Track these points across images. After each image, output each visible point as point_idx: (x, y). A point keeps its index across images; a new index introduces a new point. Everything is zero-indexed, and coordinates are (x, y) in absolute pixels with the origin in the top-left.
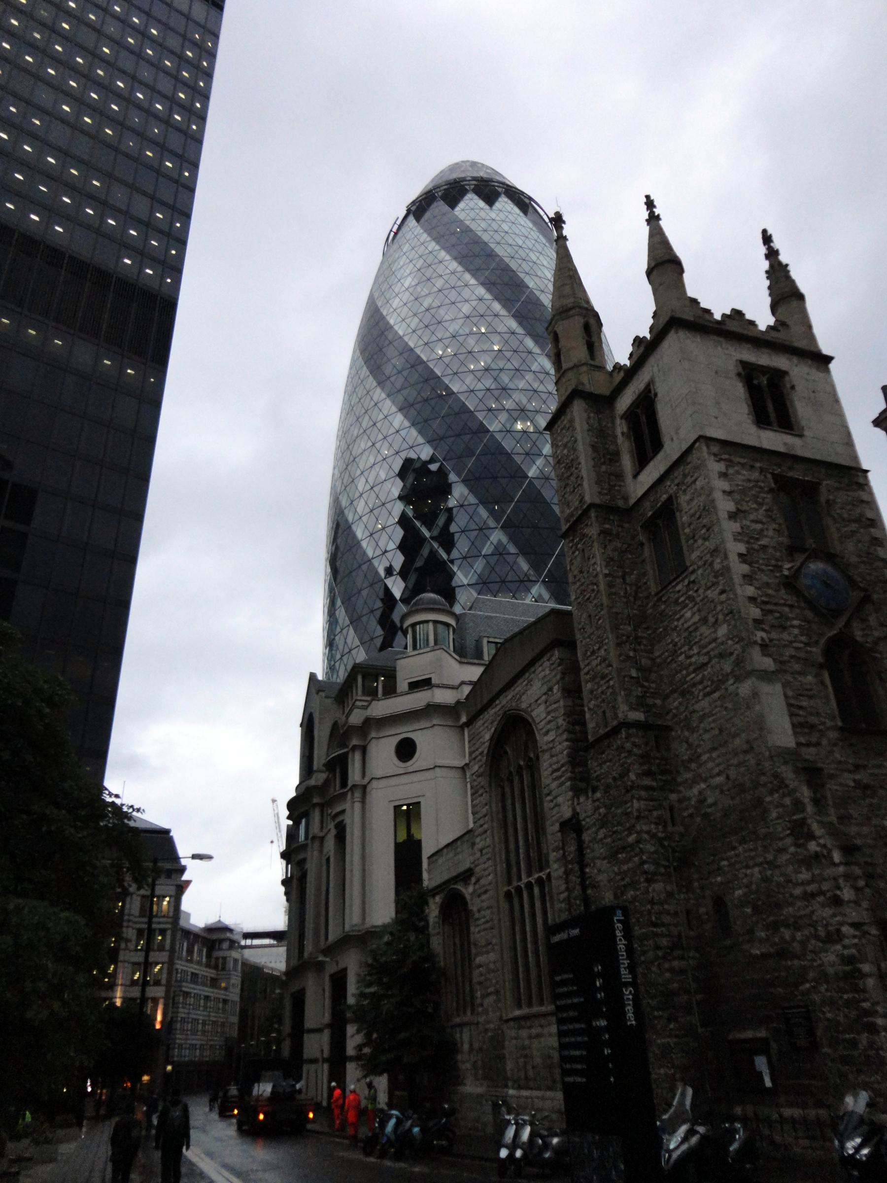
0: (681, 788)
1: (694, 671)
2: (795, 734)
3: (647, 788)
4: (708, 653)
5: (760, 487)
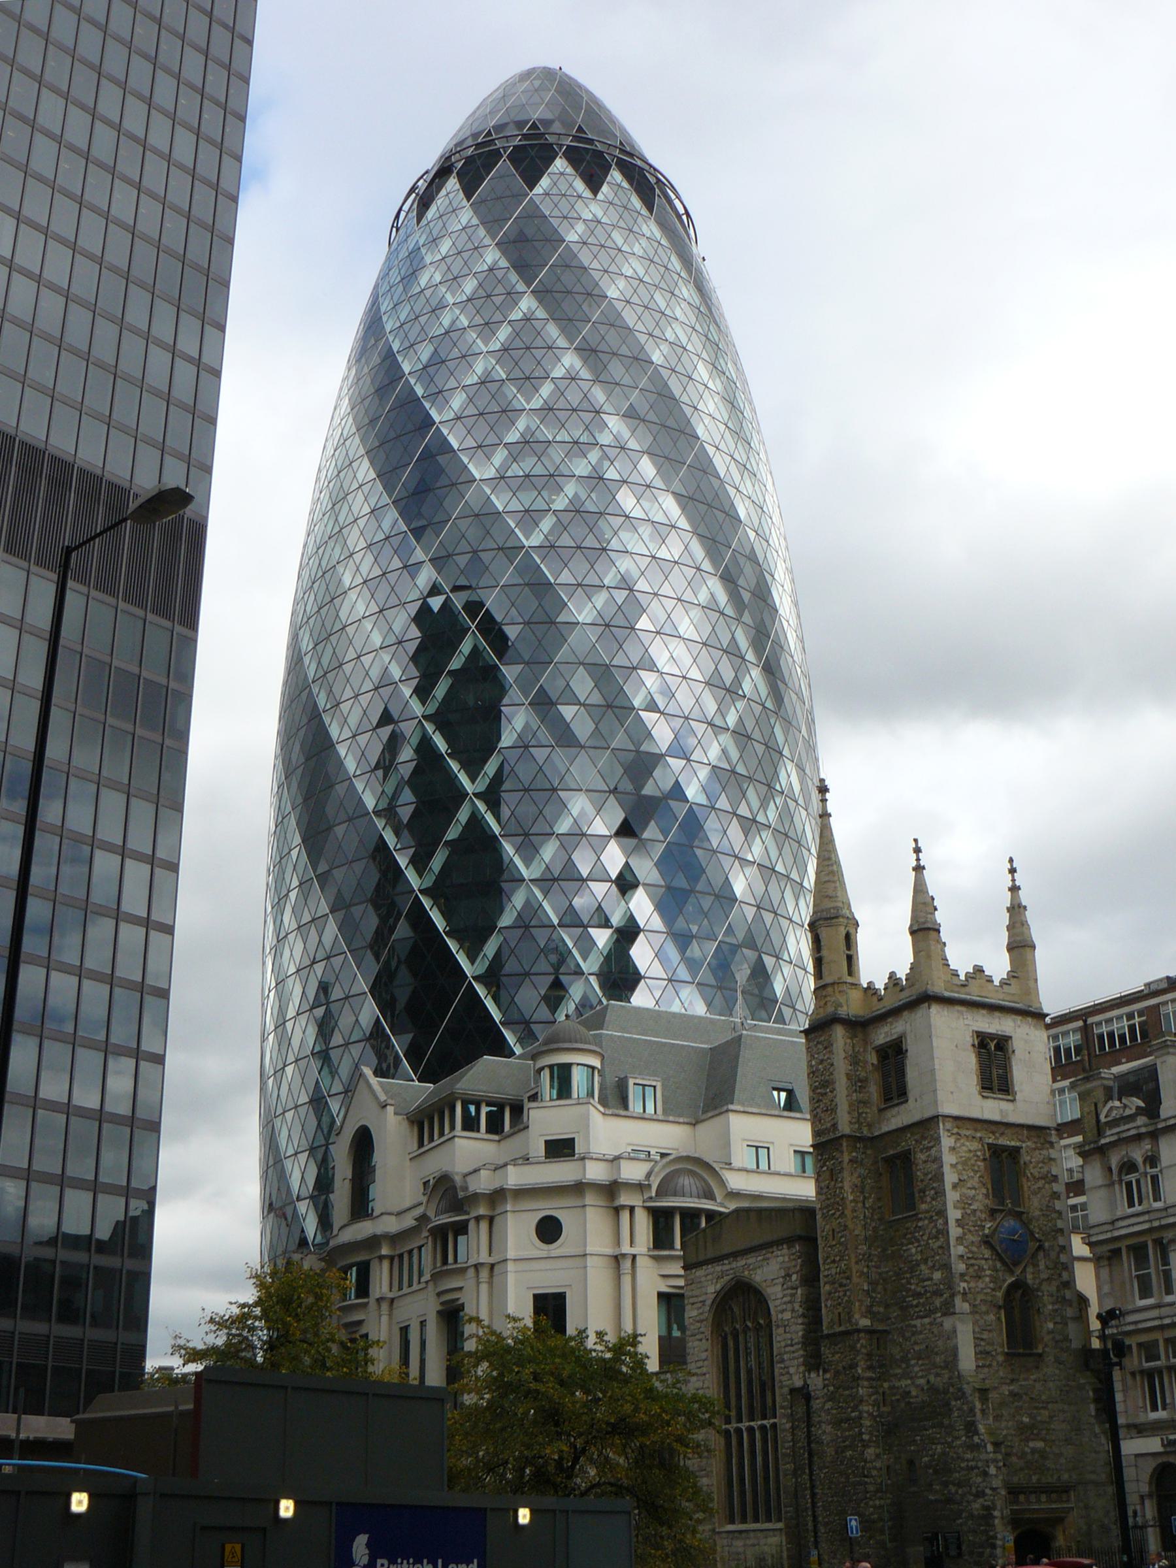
0: (892, 1378)
1: (913, 1296)
2: (977, 1359)
3: (870, 1379)
4: (924, 1287)
5: (977, 1156)
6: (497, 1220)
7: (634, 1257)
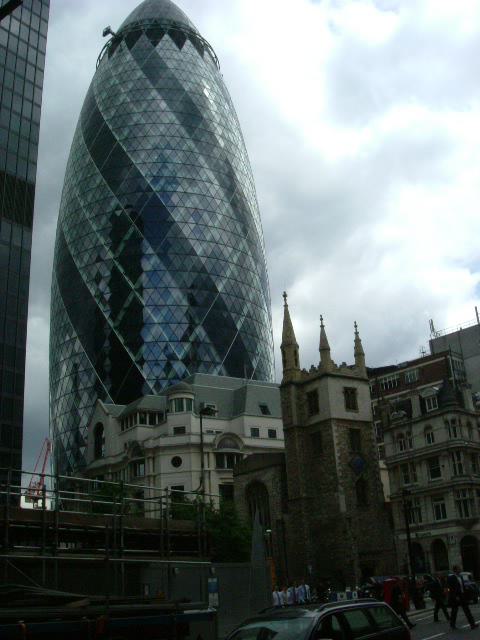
6: (156, 460)
7: (209, 472)
